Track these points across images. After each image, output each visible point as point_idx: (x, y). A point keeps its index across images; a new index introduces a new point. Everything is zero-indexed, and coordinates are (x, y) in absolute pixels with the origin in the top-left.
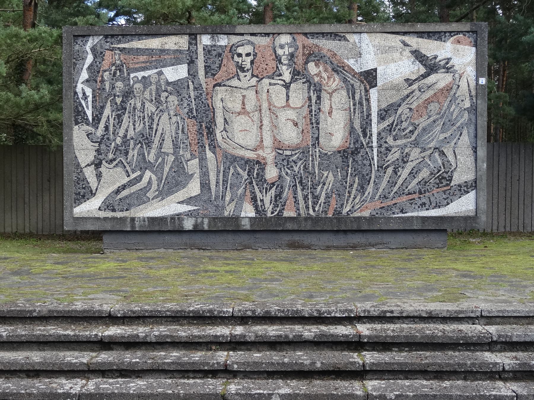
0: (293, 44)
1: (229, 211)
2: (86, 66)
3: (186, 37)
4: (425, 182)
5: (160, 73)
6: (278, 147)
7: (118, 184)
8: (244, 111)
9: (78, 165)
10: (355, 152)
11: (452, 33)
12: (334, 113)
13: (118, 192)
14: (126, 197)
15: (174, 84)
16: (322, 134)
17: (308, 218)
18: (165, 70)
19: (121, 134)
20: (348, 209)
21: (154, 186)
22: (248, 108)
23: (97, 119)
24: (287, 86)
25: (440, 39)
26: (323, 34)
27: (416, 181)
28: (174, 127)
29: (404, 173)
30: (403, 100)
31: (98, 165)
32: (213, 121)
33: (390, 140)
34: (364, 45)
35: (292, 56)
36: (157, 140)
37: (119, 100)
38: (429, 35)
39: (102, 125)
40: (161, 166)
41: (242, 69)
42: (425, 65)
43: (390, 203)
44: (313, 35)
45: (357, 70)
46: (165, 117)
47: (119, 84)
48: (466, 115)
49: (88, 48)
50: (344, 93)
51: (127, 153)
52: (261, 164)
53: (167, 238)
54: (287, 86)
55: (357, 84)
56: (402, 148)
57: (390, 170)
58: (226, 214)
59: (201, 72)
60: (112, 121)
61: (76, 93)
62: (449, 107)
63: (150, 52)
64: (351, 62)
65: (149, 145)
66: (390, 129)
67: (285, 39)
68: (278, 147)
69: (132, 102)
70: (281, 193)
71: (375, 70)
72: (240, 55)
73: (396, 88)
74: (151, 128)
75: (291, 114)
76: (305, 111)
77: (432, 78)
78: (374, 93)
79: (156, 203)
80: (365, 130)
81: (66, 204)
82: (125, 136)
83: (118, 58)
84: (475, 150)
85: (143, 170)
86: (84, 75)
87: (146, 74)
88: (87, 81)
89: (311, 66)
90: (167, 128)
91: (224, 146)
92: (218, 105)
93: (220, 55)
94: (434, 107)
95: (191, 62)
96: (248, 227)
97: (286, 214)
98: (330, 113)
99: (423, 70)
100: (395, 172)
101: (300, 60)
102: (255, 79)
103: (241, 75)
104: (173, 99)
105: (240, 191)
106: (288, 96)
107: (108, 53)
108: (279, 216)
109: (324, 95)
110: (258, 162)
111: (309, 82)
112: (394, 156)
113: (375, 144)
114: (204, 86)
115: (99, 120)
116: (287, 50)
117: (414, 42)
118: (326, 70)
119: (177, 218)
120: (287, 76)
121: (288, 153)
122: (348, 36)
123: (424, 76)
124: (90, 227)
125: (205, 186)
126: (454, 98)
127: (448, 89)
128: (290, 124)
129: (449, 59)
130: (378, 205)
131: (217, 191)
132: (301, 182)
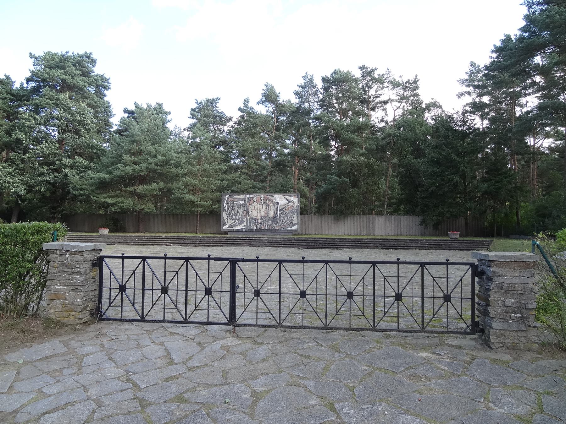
6: (261, 216)
8: (255, 209)
10: (275, 217)
13: (231, 224)
17: (266, 229)
24: (263, 205)
29: (284, 221)
33: (281, 215)
38: (289, 196)
43: (281, 227)
53: (240, 233)
54: (263, 205)
55: (275, 205)
59: (247, 202)
64: (274, 201)
66: (282, 213)
67: (262, 196)
68: (261, 216)
73: (283, 205)
81: (222, 226)
86: (225, 202)
89: (267, 201)
99: (288, 202)
101: (265, 200)
104: (242, 207)
112: (282, 218)
116: (263, 198)
117: (286, 197)
120: (263, 203)
123: (288, 203)
125: (247, 223)
126: (294, 207)
130: (279, 227)
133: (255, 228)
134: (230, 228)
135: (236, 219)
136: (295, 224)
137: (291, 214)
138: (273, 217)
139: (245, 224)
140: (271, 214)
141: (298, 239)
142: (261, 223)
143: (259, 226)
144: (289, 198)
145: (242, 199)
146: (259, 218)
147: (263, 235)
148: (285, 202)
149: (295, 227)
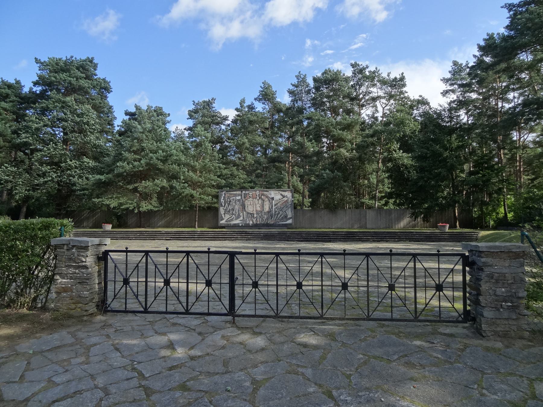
1: (248, 223)
4: (282, 217)
6: (256, 211)
8: (250, 205)
10: (270, 212)
17: (262, 224)
29: (279, 216)
31: (225, 214)
38: (283, 191)
52: (254, 214)
56: (279, 211)
64: (269, 196)
66: (276, 208)
67: (258, 192)
68: (256, 211)
73: (277, 200)
77: (284, 199)
78: (273, 201)
80: (272, 208)
83: (229, 195)
86: (223, 198)
95: (241, 196)
101: (260, 196)
104: (238, 202)
108: (257, 224)
111: (262, 199)
112: (277, 213)
117: (281, 192)
119: (239, 224)
120: (258, 198)
125: (243, 218)
127: (287, 200)
133: (251, 223)
135: (233, 214)
136: (290, 218)
137: (285, 209)
138: (268, 212)
139: (242, 218)
140: (267, 208)
141: (292, 233)
142: (257, 217)
144: (283, 193)
145: (239, 195)
146: (255, 212)
147: (259, 229)
148: (280, 197)
149: (290, 221)
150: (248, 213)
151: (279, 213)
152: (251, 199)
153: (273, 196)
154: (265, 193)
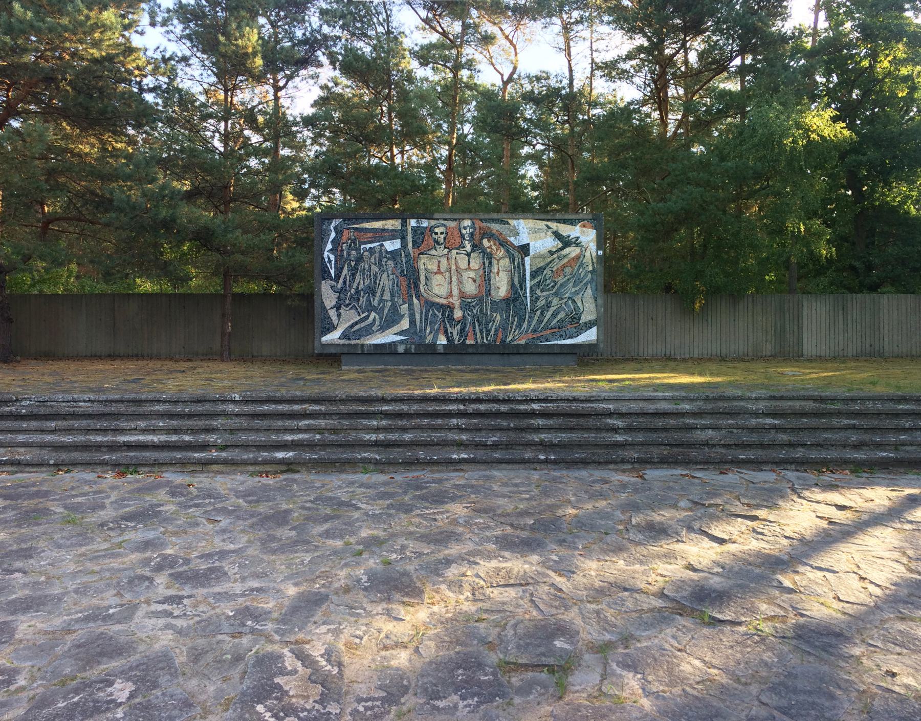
0: (473, 226)
1: (429, 339)
2: (330, 240)
3: (400, 221)
5: (382, 245)
6: (462, 295)
7: (352, 321)
8: (439, 272)
9: (325, 307)
11: (580, 220)
12: (501, 273)
13: (352, 326)
14: (358, 330)
15: (391, 252)
16: (492, 288)
17: (483, 345)
18: (385, 243)
19: (355, 287)
20: (510, 338)
21: (378, 323)
22: (442, 269)
23: (338, 276)
25: (572, 224)
26: (494, 220)
27: (556, 320)
28: (391, 283)
29: (548, 315)
30: (547, 265)
32: (418, 278)
33: (538, 292)
34: (521, 228)
35: (472, 234)
36: (379, 292)
37: (353, 264)
38: (564, 221)
39: (341, 281)
40: (382, 309)
41: (438, 243)
42: (561, 242)
44: (487, 220)
45: (516, 243)
46: (385, 276)
47: (354, 252)
48: (590, 275)
49: (332, 228)
50: (507, 260)
51: (358, 300)
52: (451, 308)
53: (386, 358)
54: (469, 255)
55: (516, 254)
56: (547, 297)
57: (539, 312)
58: (427, 342)
59: (410, 245)
60: (348, 277)
61: (323, 258)
62: (578, 270)
63: (374, 231)
64: (512, 239)
65: (374, 294)
66: (538, 285)
67: (467, 223)
69: (362, 265)
70: (465, 327)
71: (528, 244)
72: (436, 234)
73: (542, 257)
74: (375, 283)
75: (472, 274)
76: (481, 272)
78: (527, 260)
79: (379, 335)
81: (317, 335)
82: (358, 288)
83: (352, 234)
84: (596, 299)
85: (369, 311)
86: (329, 246)
87: (372, 245)
88: (331, 250)
90: (386, 283)
91: (425, 295)
92: (422, 267)
93: (423, 233)
94: (568, 270)
95: (403, 239)
96: (442, 351)
97: (468, 342)
98: (498, 273)
99: (560, 245)
100: (542, 314)
101: (477, 237)
102: (446, 250)
103: (437, 247)
104: (391, 263)
105: (436, 327)
106: (469, 262)
107: (346, 232)
109: (494, 261)
110: (449, 307)
111: (484, 252)
113: (528, 295)
114: (412, 254)
115: (339, 277)
116: (468, 231)
117: (554, 225)
118: (495, 244)
120: (468, 248)
121: (469, 300)
122: (510, 221)
123: (562, 249)
124: (333, 351)
125: (412, 322)
126: (582, 264)
127: (578, 258)
128: (470, 280)
129: (578, 238)
131: (421, 326)
132: (478, 320)
133: (442, 340)
134: (346, 342)
135: (370, 308)
136: (589, 325)
137: (571, 289)
138: (507, 301)
139: (405, 324)
143: (455, 333)
144: (566, 230)
146: (456, 301)
148: (550, 243)
149: (590, 336)
150: (430, 305)
151: (548, 305)
152: (443, 251)
153: (524, 239)
154: (495, 227)
